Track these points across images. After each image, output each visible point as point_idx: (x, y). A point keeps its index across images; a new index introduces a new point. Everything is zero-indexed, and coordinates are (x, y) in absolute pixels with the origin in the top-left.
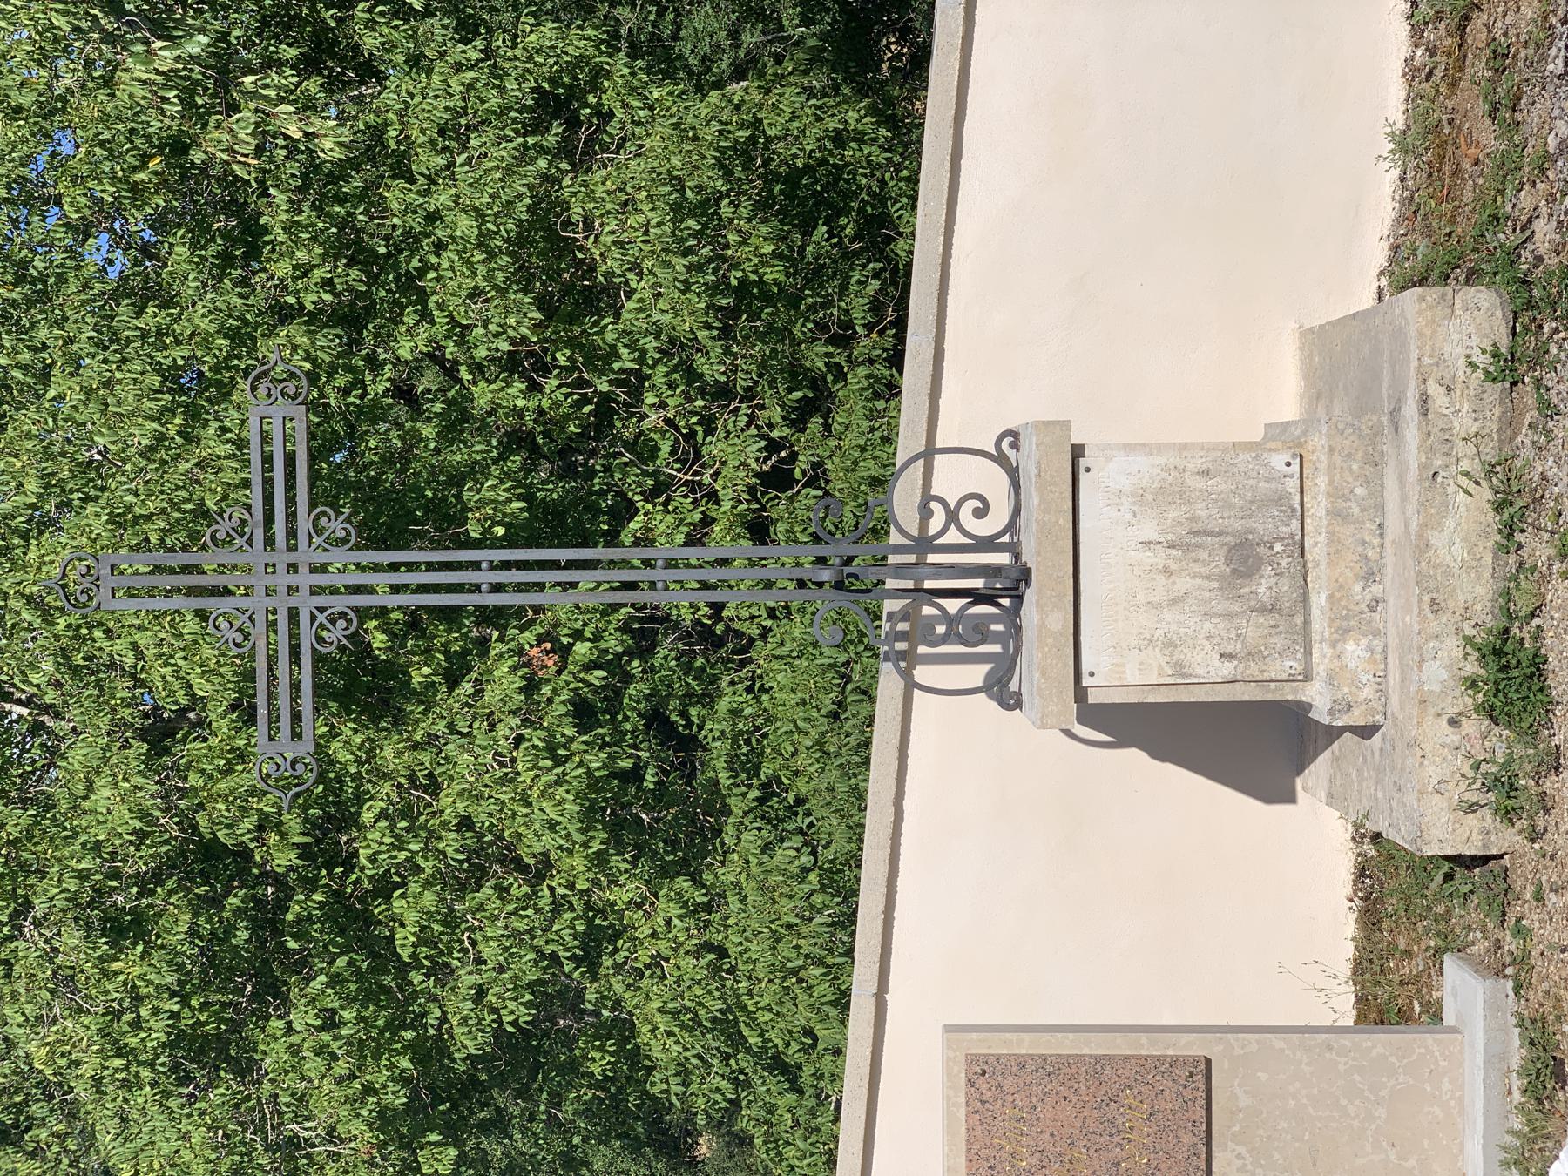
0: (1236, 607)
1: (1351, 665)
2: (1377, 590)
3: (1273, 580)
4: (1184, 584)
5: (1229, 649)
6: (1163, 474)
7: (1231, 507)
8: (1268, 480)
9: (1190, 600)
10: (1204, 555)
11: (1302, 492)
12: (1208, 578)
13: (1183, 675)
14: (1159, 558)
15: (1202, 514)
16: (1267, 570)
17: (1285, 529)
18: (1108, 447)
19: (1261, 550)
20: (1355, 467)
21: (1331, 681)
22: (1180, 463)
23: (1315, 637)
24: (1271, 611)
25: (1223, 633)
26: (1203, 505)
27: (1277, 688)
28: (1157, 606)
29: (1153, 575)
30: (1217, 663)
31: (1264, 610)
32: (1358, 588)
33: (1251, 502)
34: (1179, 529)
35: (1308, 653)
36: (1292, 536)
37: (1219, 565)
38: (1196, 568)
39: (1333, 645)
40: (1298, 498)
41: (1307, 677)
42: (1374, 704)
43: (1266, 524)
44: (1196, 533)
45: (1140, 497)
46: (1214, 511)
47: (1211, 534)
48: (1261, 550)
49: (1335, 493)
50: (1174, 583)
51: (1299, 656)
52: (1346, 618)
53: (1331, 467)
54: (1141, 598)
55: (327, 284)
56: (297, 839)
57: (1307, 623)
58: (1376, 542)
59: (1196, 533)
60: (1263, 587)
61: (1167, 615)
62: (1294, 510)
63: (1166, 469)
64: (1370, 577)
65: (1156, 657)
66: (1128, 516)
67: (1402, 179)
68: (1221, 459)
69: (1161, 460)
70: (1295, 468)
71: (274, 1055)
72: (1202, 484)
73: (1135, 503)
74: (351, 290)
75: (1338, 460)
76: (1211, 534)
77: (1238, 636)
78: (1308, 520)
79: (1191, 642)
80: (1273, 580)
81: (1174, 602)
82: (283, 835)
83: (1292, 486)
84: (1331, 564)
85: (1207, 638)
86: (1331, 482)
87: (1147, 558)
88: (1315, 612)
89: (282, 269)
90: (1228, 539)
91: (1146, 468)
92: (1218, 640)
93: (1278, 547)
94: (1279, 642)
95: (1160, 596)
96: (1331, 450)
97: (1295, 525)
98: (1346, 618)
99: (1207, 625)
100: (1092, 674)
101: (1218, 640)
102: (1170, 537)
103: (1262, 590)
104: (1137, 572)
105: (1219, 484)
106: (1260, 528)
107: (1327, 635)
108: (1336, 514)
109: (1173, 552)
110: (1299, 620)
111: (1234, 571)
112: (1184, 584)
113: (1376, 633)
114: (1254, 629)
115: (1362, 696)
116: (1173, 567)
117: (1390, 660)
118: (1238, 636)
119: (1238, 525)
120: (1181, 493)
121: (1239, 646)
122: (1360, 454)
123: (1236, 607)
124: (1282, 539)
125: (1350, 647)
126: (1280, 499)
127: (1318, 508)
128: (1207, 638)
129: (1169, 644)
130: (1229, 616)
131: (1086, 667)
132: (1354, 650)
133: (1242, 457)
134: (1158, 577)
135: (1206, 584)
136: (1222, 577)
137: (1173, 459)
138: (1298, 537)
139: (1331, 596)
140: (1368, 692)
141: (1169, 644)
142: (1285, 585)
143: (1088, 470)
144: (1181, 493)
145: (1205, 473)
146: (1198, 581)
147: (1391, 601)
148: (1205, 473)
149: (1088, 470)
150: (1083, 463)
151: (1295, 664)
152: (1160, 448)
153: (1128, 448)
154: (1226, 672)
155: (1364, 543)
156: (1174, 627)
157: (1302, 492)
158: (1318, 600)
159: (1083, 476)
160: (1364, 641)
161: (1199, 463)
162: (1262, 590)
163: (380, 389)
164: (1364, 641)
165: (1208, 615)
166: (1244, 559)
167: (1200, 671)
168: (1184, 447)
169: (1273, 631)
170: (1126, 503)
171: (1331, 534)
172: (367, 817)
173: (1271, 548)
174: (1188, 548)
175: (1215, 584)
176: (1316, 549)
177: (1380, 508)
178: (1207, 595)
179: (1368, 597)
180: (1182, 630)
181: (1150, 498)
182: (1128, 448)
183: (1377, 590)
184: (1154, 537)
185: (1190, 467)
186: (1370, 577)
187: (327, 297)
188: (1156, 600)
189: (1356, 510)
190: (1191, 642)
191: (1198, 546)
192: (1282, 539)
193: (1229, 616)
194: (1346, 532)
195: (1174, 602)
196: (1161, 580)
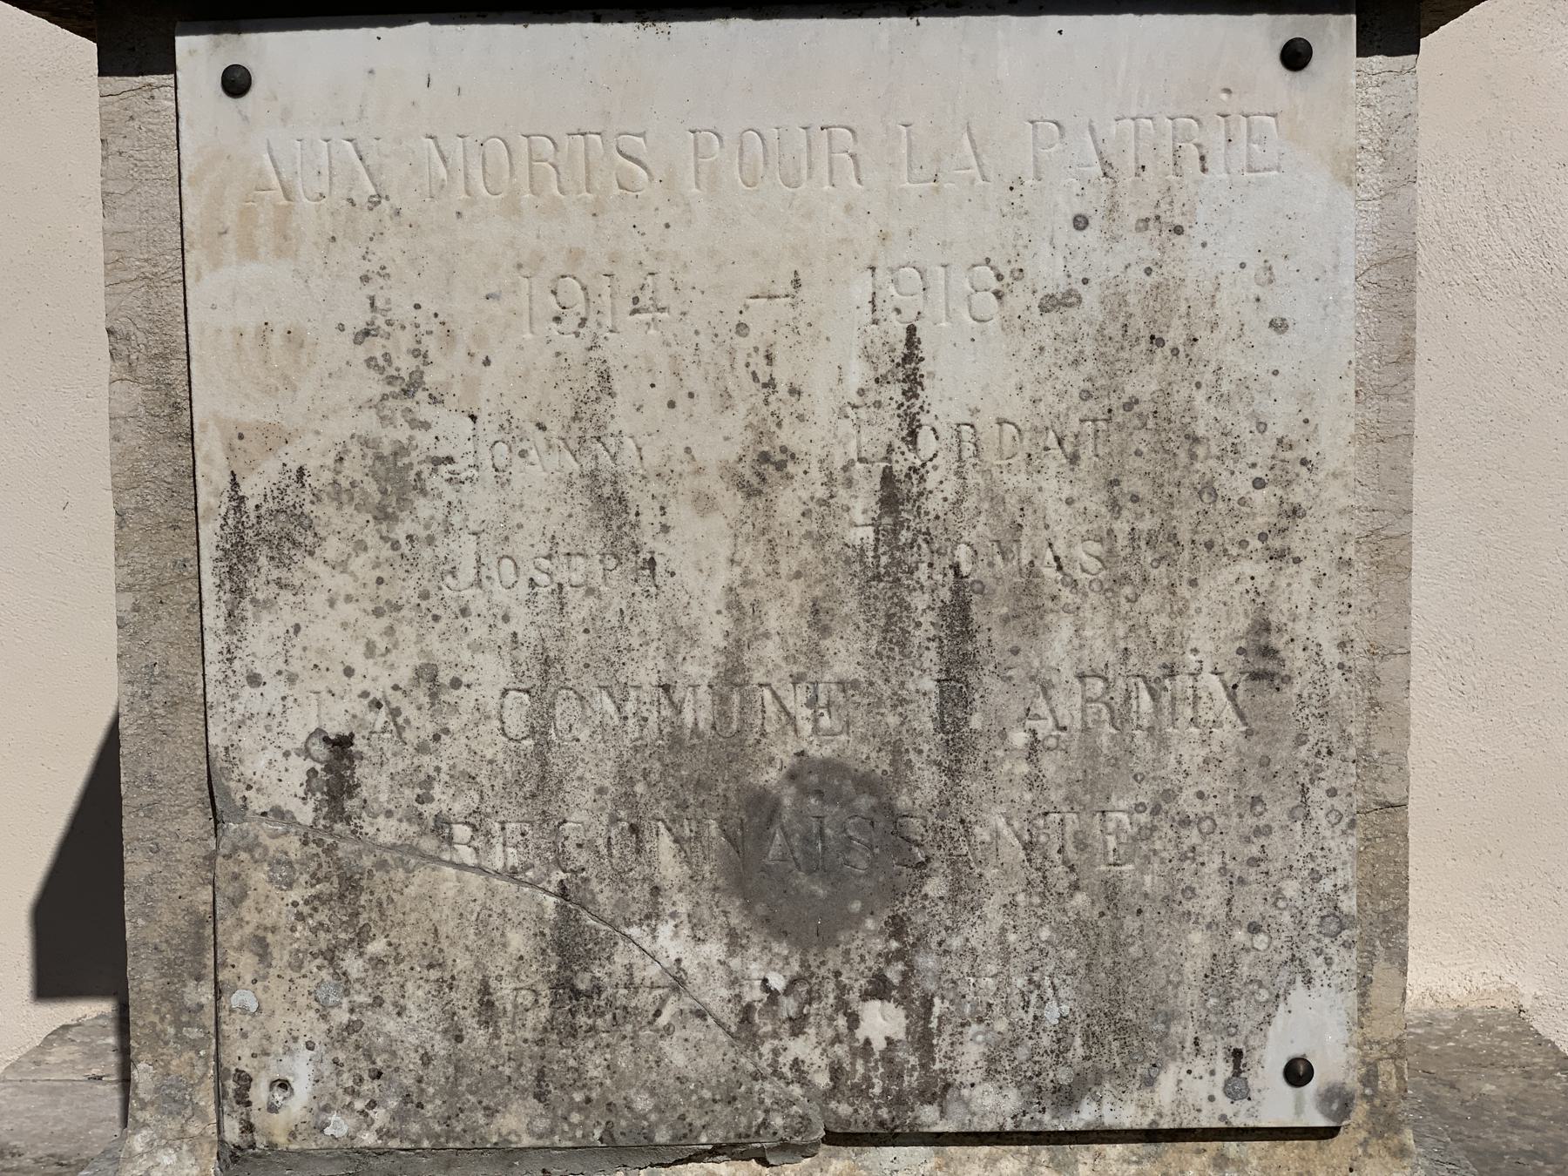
0: (583, 815)
3: (716, 996)
5: (373, 781)
6: (1260, 450)
7: (1090, 790)
8: (1220, 976)
9: (617, 588)
10: (846, 656)
11: (1151, 1136)
12: (732, 675)
13: (237, 555)
14: (836, 429)
15: (1057, 647)
16: (767, 968)
17: (972, 1052)
18: (1401, 176)
22: (1312, 541)
24: (566, 991)
25: (453, 751)
26: (1101, 651)
27: (185, 1014)
28: (587, 420)
29: (746, 395)
30: (301, 724)
31: (570, 949)
33: (1111, 893)
34: (981, 531)
36: (938, 1091)
37: (798, 731)
38: (782, 618)
40: (1128, 1116)
44: (958, 616)
46: (1069, 707)
47: (956, 692)
50: (704, 503)
51: (339, 1126)
54: (630, 342)
59: (958, 616)
60: (684, 950)
61: (543, 473)
62: (1067, 1098)
63: (1290, 462)
65: (330, 417)
66: (1048, 272)
68: (1320, 731)
69: (1335, 439)
70: (1278, 1105)
72: (1210, 637)
73: (1116, 302)
76: (956, 692)
77: (441, 825)
79: (407, 591)
80: (716, 996)
81: (610, 504)
83: (1188, 1089)
85: (427, 674)
87: (834, 371)
90: (927, 782)
91: (1296, 372)
92: (421, 725)
93: (882, 1022)
94: (410, 1027)
95: (641, 433)
97: (994, 1104)
99: (491, 673)
100: (236, 83)
101: (421, 725)
102: (940, 484)
103: (670, 942)
104: (762, 318)
105: (1202, 737)
106: (978, 935)
109: (862, 503)
111: (762, 805)
112: (701, 554)
114: (474, 903)
116: (788, 502)
118: (441, 825)
119: (997, 825)
120: (1165, 541)
121: (387, 831)
123: (583, 815)
124: (923, 1041)
126: (1124, 1031)
128: (427, 674)
129: (395, 482)
130: (541, 782)
133: (1342, 847)
134: (734, 424)
135: (700, 669)
136: (733, 743)
137: (1334, 505)
138: (928, 1117)
141: (395, 482)
142: (694, 1054)
143: (1295, 56)
144: (1165, 541)
145: (1262, 661)
146: (715, 631)
148: (1262, 661)
149: (1295, 56)
151: (297, 1105)
152: (1388, 440)
153: (1392, 279)
154: (256, 764)
156: (482, 503)
157: (1151, 1136)
161: (1314, 624)
162: (670, 942)
165: (544, 674)
168: (1385, 554)
169: (464, 998)
170: (1115, 260)
173: (879, 989)
174: (885, 573)
175: (698, 711)
178: (645, 672)
180: (464, 550)
181: (1143, 383)
182: (1392, 279)
184: (943, 402)
185: (1295, 590)
188: (621, 416)
190: (407, 591)
191: (894, 633)
192: (923, 1041)
193: (541, 782)
195: (610, 504)
196: (722, 441)
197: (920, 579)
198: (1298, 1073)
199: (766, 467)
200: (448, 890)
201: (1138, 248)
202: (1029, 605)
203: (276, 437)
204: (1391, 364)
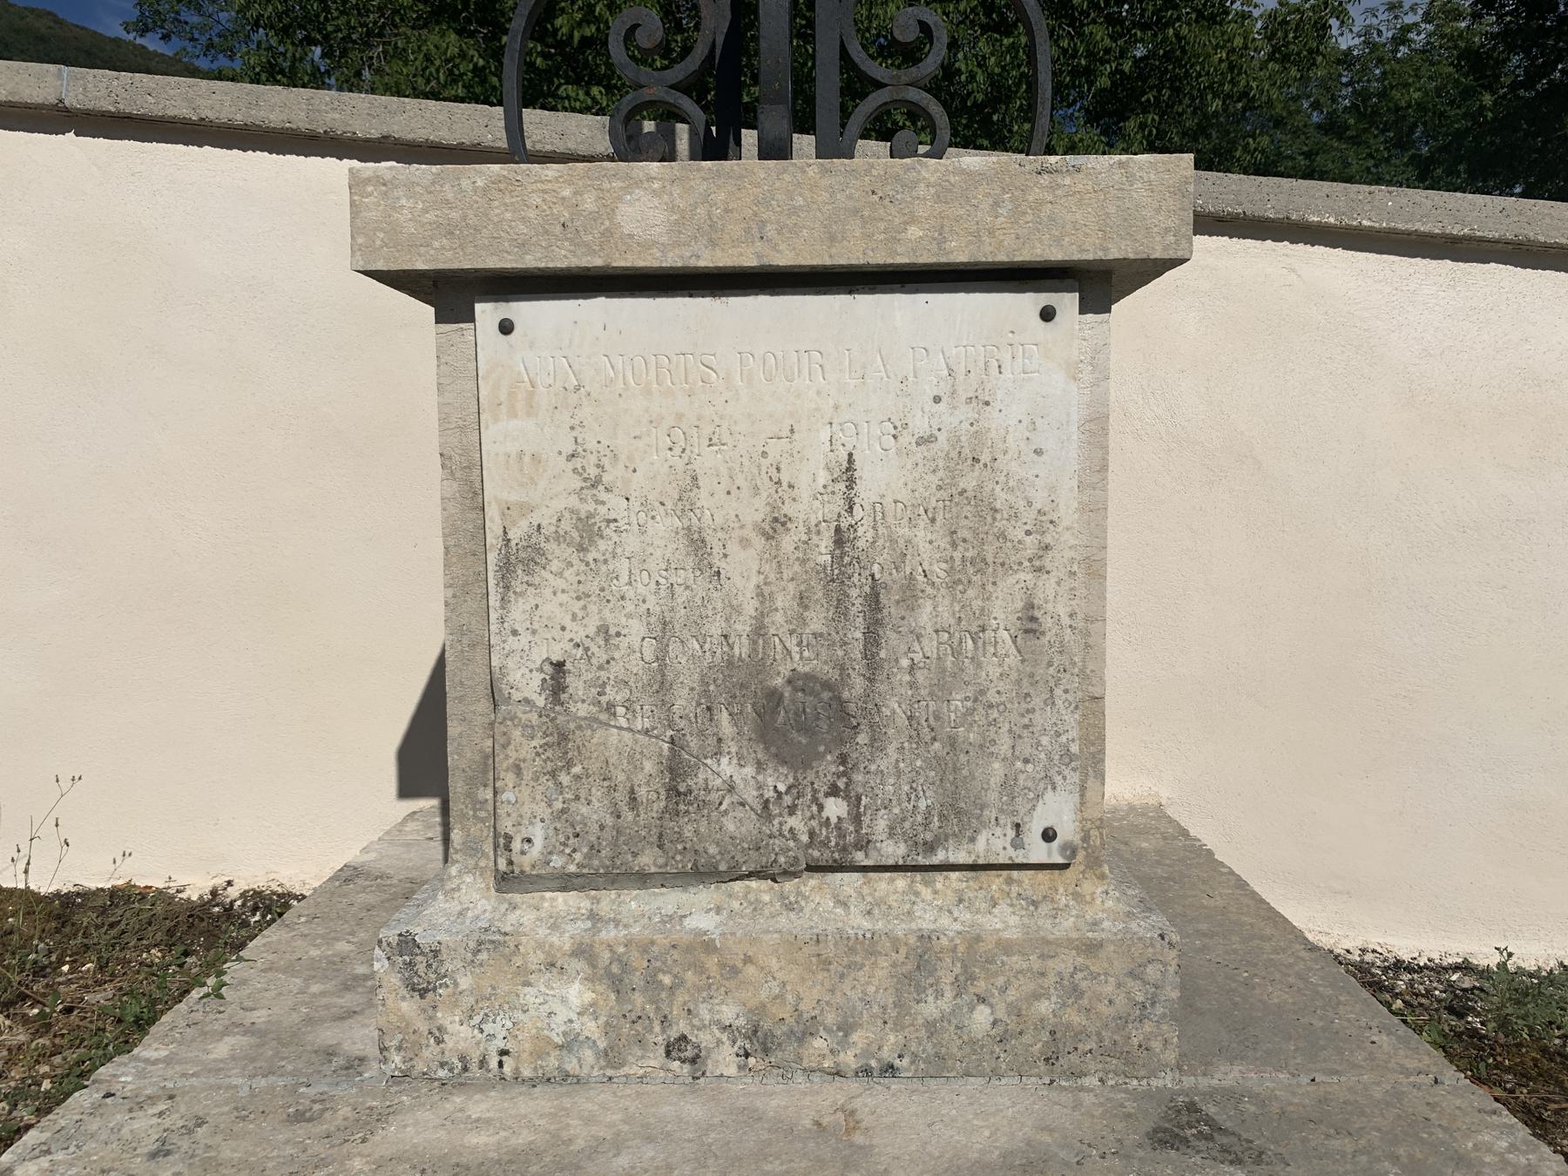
0: (683, 701)
1: (529, 996)
2: (725, 1060)
3: (750, 795)
4: (743, 568)
5: (575, 685)
6: (1029, 516)
7: (941, 689)
8: (1008, 785)
9: (701, 585)
10: (817, 620)
12: (759, 631)
13: (506, 569)
14: (812, 506)
15: (924, 616)
16: (777, 780)
17: (882, 824)
18: (1102, 375)
19: (828, 766)
20: (1044, 1007)
21: (491, 944)
23: (607, 901)
24: (673, 792)
25: (616, 669)
26: (947, 619)
27: (479, 804)
28: (685, 500)
29: (767, 488)
30: (539, 655)
31: (676, 770)
32: (728, 1013)
33: (952, 742)
34: (885, 557)
35: (565, 882)
36: (864, 844)
37: (793, 657)
38: (784, 600)
39: (582, 951)
40: (961, 857)
41: (507, 881)
42: (430, 1052)
43: (892, 774)
44: (873, 601)
45: (973, 454)
46: (930, 646)
47: (872, 638)
48: (828, 766)
49: (976, 961)
50: (745, 543)
51: (557, 862)
52: (651, 982)
53: (1047, 948)
54: (708, 461)
55: (972, 76)
56: (576, 35)
57: (643, 879)
58: (849, 1059)
59: (873, 601)
60: (733, 770)
61: (664, 527)
62: (930, 848)
63: (1045, 521)
64: (758, 1042)
65: (554, 499)
66: (920, 425)
67: (1398, 965)
68: (1059, 662)
69: (1068, 510)
70: (1039, 852)
71: (432, 38)
72: (1003, 611)
73: (955, 440)
74: (969, 94)
75: (1065, 962)
76: (872, 638)
77: (610, 708)
78: (901, 881)
79: (593, 586)
80: (750, 795)
81: (697, 543)
82: (580, 24)
83: (993, 844)
84: (792, 943)
85: (603, 630)
86: (1007, 947)
87: (811, 475)
88: (669, 900)
89: (983, 46)
90: (858, 684)
91: (1047, 477)
92: (600, 655)
93: (835, 808)
94: (594, 811)
95: (713, 507)
96: (1091, 948)
97: (893, 851)
98: (651, 982)
99: (635, 630)
100: (506, 328)
101: (600, 655)
102: (865, 534)
103: (727, 767)
104: (774, 449)
105: (1000, 662)
106: (884, 764)
107: (609, 934)
108: (921, 961)
109: (825, 543)
110: (648, 860)
111: (774, 696)
112: (743, 568)
113: (611, 1057)
114: (626, 747)
115: (446, 1018)
116: (788, 542)
117: (536, 1106)
118: (610, 708)
119: (894, 707)
120: (979, 563)
121: (582, 710)
122: (1075, 1018)
123: (683, 701)
124: (857, 819)
125: (577, 993)
126: (959, 814)
127: (935, 909)
128: (603, 630)
129: (587, 531)
130: (661, 684)
131: (524, 311)
132: (569, 1002)
133: (1071, 719)
134: (760, 502)
135: (743, 627)
136: (759, 665)
137: (1067, 542)
138: (859, 857)
139: (709, 947)
140: (461, 1035)
141: (587, 531)
142: (737, 824)
143: (1047, 314)
144: (979, 563)
145: (1030, 623)
146: (750, 607)
147: (694, 1110)
148: (1030, 623)
149: (1047, 314)
150: (1067, 302)
152: (1095, 511)
153: (1097, 427)
154: (515, 676)
155: (846, 1028)
156: (632, 543)
158: (701, 911)
159: (1027, 303)
160: (591, 1028)
161: (1057, 605)
162: (727, 767)
163: (898, 117)
164: (591, 1028)
165: (663, 630)
166: (805, 722)
167: (518, 612)
168: (1093, 569)
169: (621, 796)
170: (954, 418)
171: (868, 946)
172: (595, 91)
173: (834, 791)
174: (836, 579)
175: (741, 649)
176: (834, 905)
177: (937, 1067)
178: (715, 628)
179: (705, 1039)
180: (622, 566)
181: (969, 482)
182: (1097, 427)
183: (725, 1060)
184: (866, 492)
185: (1047, 588)
186: (758, 1042)
187: (963, 78)
188: (703, 499)
189: (931, 1008)
190: (593, 586)
191: (841, 608)
193: (661, 684)
194: (877, 980)
195: (697, 543)
196: (754, 511)
197: (855, 582)
198: (1049, 835)
199: (777, 524)
200: (613, 740)
201: (966, 412)
202: (910, 595)
203: (527, 509)
204: (1097, 469)
